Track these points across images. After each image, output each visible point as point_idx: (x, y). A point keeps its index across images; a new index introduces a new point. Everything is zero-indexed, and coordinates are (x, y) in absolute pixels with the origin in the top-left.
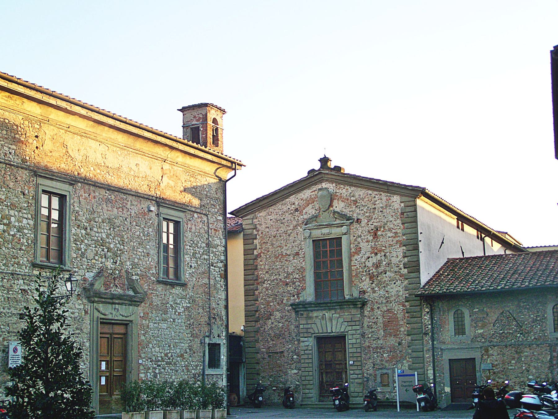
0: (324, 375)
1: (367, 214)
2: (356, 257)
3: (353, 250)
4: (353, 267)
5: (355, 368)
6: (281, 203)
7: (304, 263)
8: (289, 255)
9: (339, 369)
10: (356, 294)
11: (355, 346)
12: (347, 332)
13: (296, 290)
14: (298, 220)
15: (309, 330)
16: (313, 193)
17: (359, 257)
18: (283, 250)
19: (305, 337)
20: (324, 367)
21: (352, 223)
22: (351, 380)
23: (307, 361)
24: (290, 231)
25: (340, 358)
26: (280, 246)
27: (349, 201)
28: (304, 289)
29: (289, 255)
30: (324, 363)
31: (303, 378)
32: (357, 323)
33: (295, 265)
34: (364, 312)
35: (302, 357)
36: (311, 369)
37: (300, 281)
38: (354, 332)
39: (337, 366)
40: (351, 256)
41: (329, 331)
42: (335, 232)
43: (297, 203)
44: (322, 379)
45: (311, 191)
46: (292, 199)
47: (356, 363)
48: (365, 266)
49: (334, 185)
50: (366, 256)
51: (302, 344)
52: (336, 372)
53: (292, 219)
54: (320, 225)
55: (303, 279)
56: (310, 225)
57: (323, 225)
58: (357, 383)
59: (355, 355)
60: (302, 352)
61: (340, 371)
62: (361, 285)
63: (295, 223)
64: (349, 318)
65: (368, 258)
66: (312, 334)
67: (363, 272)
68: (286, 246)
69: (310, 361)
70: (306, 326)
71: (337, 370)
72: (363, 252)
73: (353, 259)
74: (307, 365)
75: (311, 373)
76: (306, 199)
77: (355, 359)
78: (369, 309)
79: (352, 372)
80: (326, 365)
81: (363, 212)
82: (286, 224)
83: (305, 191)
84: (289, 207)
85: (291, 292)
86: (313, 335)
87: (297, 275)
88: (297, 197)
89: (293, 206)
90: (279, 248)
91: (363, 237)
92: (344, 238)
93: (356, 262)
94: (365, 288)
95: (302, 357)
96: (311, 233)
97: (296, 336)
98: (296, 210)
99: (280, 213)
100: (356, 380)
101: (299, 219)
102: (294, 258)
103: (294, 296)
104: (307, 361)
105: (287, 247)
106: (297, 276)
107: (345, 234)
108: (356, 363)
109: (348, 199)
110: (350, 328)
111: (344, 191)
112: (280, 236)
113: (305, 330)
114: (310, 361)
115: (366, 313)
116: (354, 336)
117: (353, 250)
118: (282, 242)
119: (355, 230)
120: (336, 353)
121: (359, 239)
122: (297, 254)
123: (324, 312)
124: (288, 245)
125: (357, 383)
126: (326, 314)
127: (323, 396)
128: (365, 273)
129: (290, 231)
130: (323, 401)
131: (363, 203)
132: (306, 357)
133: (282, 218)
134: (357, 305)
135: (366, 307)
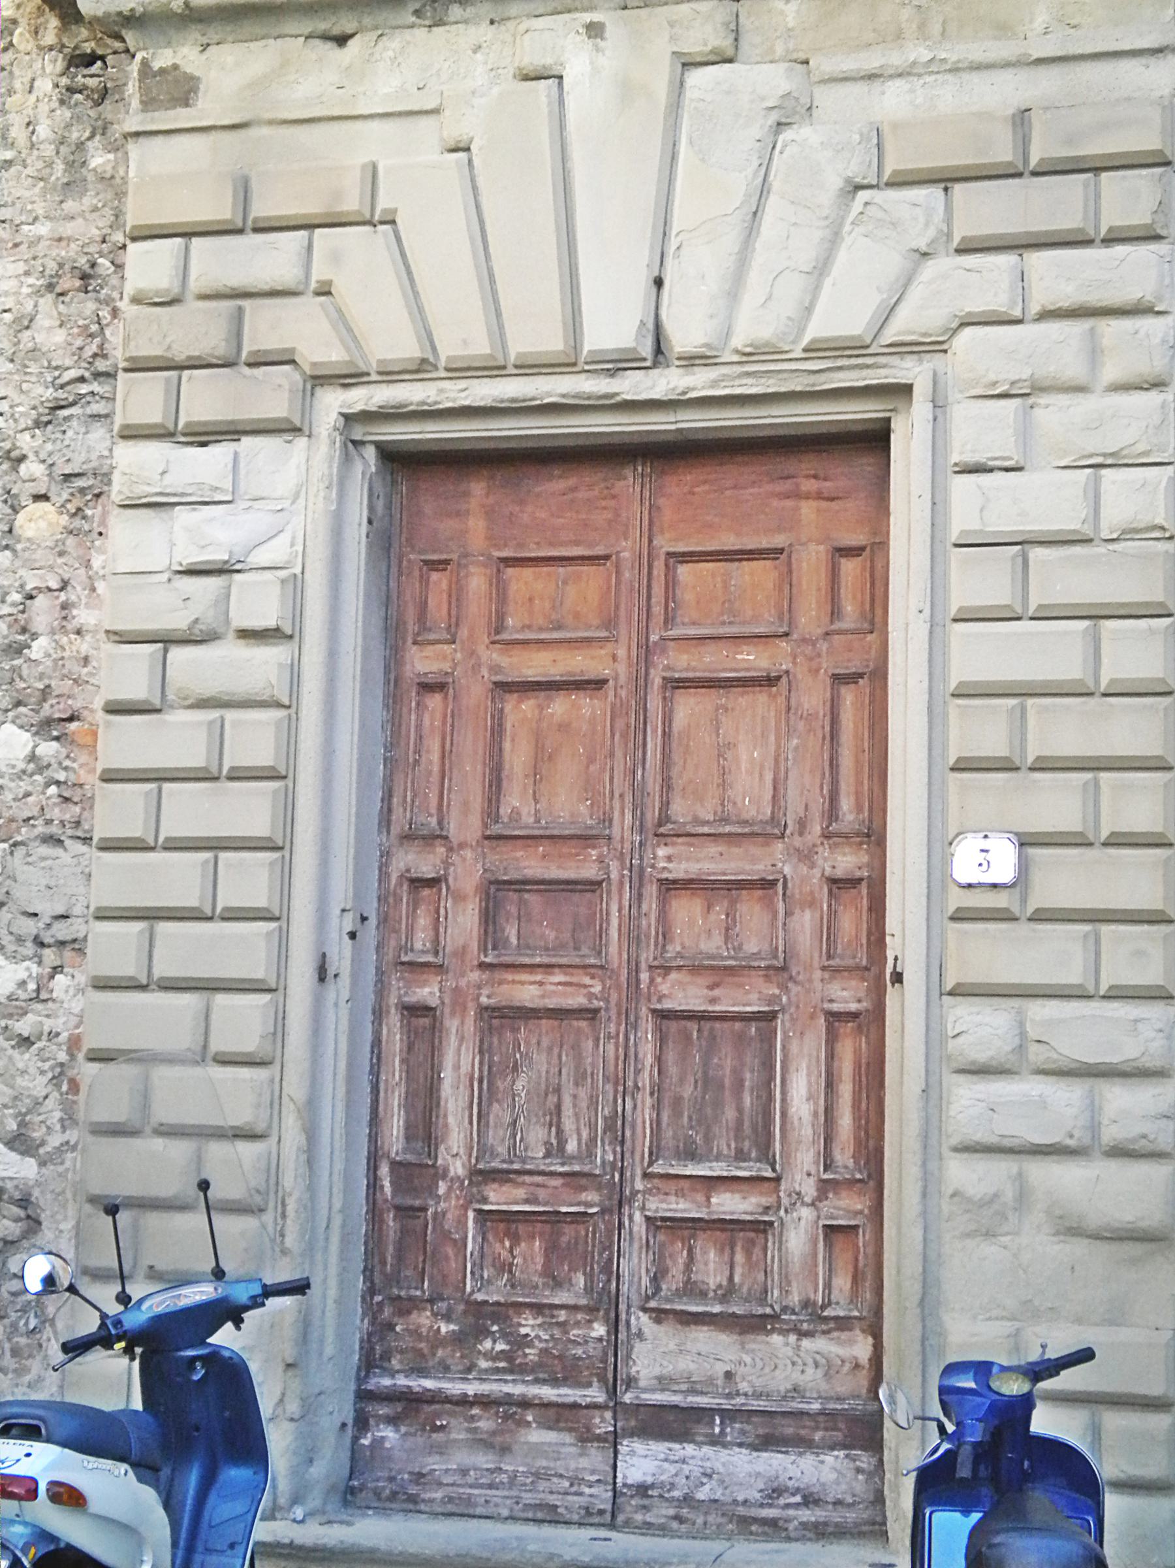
0: (458, 1060)
5: (1055, 955)
9: (721, 973)
11: (1060, 578)
12: (933, 347)
15: (267, 327)
19: (204, 436)
20: (464, 922)
22: (967, 1176)
23: (189, 811)
25: (751, 798)
30: (467, 873)
31: (107, 1093)
35: (127, 743)
36: (242, 950)
38: (1058, 348)
39: (694, 926)
41: (612, 326)
44: (425, 1128)
47: (1066, 881)
51: (133, 544)
52: (663, 1015)
58: (1072, 1229)
59: (1060, 730)
60: (129, 673)
61: (747, 998)
66: (320, 380)
69: (247, 811)
70: (213, 263)
71: (684, 994)
74: (177, 879)
75: (240, 1021)
77: (1056, 804)
79: (981, 1028)
80: (497, 892)
86: (333, 403)
95: (127, 743)
97: (49, 418)
100: (1065, 1180)
104: (189, 811)
108: (1066, 881)
110: (990, 281)
113: (196, 330)
114: (247, 811)
116: (1053, 414)
120: (687, 707)
125: (1072, 1229)
127: (410, 1406)
130: (404, 1499)
132: (177, 740)
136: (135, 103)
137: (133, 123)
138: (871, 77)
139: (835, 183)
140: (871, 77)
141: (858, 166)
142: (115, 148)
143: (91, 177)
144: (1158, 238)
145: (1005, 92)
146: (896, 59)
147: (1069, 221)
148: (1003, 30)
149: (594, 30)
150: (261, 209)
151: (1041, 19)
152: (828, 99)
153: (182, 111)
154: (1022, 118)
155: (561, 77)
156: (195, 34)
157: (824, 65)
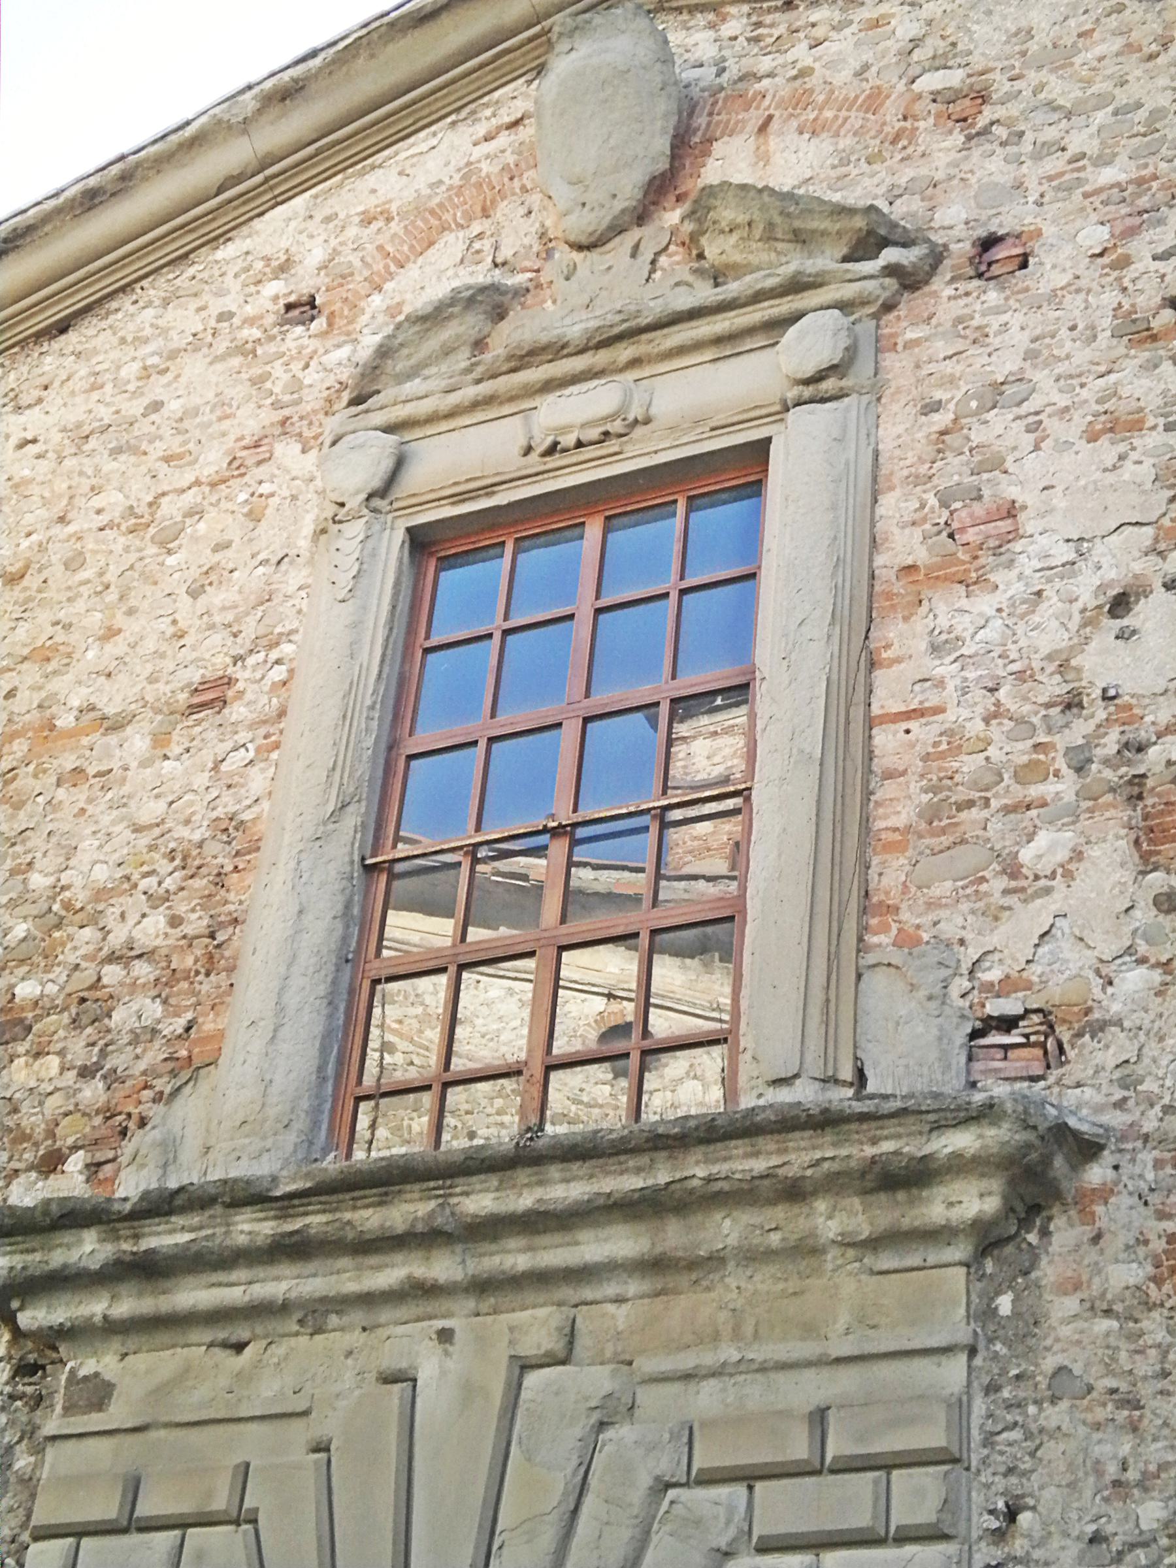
1: (1108, 175)
2: (948, 610)
3: (906, 546)
4: (885, 739)
6: (155, 289)
7: (258, 781)
8: (115, 725)
10: (909, 1049)
13: (93, 1092)
14: (296, 386)
16: (503, 139)
17: (984, 604)
18: (57, 685)
21: (910, 281)
24: (190, 498)
26: (42, 655)
27: (891, 112)
28: (188, 1065)
29: (115, 725)
32: (916, 1496)
33: (150, 810)
34: (1029, 1324)
37: (166, 985)
40: (864, 611)
42: (689, 401)
43: (317, 254)
45: (481, 130)
46: (277, 230)
48: (1072, 704)
49: (731, 28)
50: (1086, 588)
53: (238, 392)
54: (524, 358)
55: (215, 951)
56: (413, 387)
57: (557, 350)
62: (1008, 943)
63: (252, 420)
64: (762, 1411)
65: (1120, 604)
67: (1029, 773)
68: (110, 633)
72: (1042, 544)
73: (903, 637)
76: (420, 208)
78: (1126, 1275)
81: (1054, 164)
82: (158, 449)
83: (421, 142)
84: (230, 303)
85: (32, 1119)
87: (157, 921)
88: (333, 205)
89: (274, 287)
90: (31, 673)
91: (1047, 391)
92: (802, 456)
93: (945, 668)
94: (1062, 973)
96: (400, 463)
98: (303, 309)
99: (131, 370)
101: (311, 377)
102: (160, 740)
103: (51, 1163)
105: (116, 647)
106: (152, 929)
107: (818, 386)
109: (874, 101)
111: (841, 45)
112: (74, 563)
115: (1071, 1334)
117: (906, 546)
118: (80, 605)
119: (941, 348)
121: (999, 429)
122: (212, 696)
123: (407, 1340)
124: (132, 627)
126: (430, 1367)
128: (1062, 787)
129: (190, 498)
131: (1060, 90)
133: (135, 408)
134: (913, 1177)
135: (1065, 1233)
136: (59, 1408)
137: (51, 1427)
138: (687, 1377)
139: (645, 1481)
140: (687, 1377)
141: (667, 1463)
142: (38, 1450)
143: (13, 1479)
144: (946, 1537)
145: (810, 1389)
146: (709, 1359)
147: (861, 1518)
148: (809, 1330)
149: (445, 1336)
150: (146, 1508)
151: (843, 1321)
152: (647, 1397)
153: (95, 1416)
154: (819, 1418)
155: (415, 1380)
156: (116, 1344)
157: (648, 1365)
